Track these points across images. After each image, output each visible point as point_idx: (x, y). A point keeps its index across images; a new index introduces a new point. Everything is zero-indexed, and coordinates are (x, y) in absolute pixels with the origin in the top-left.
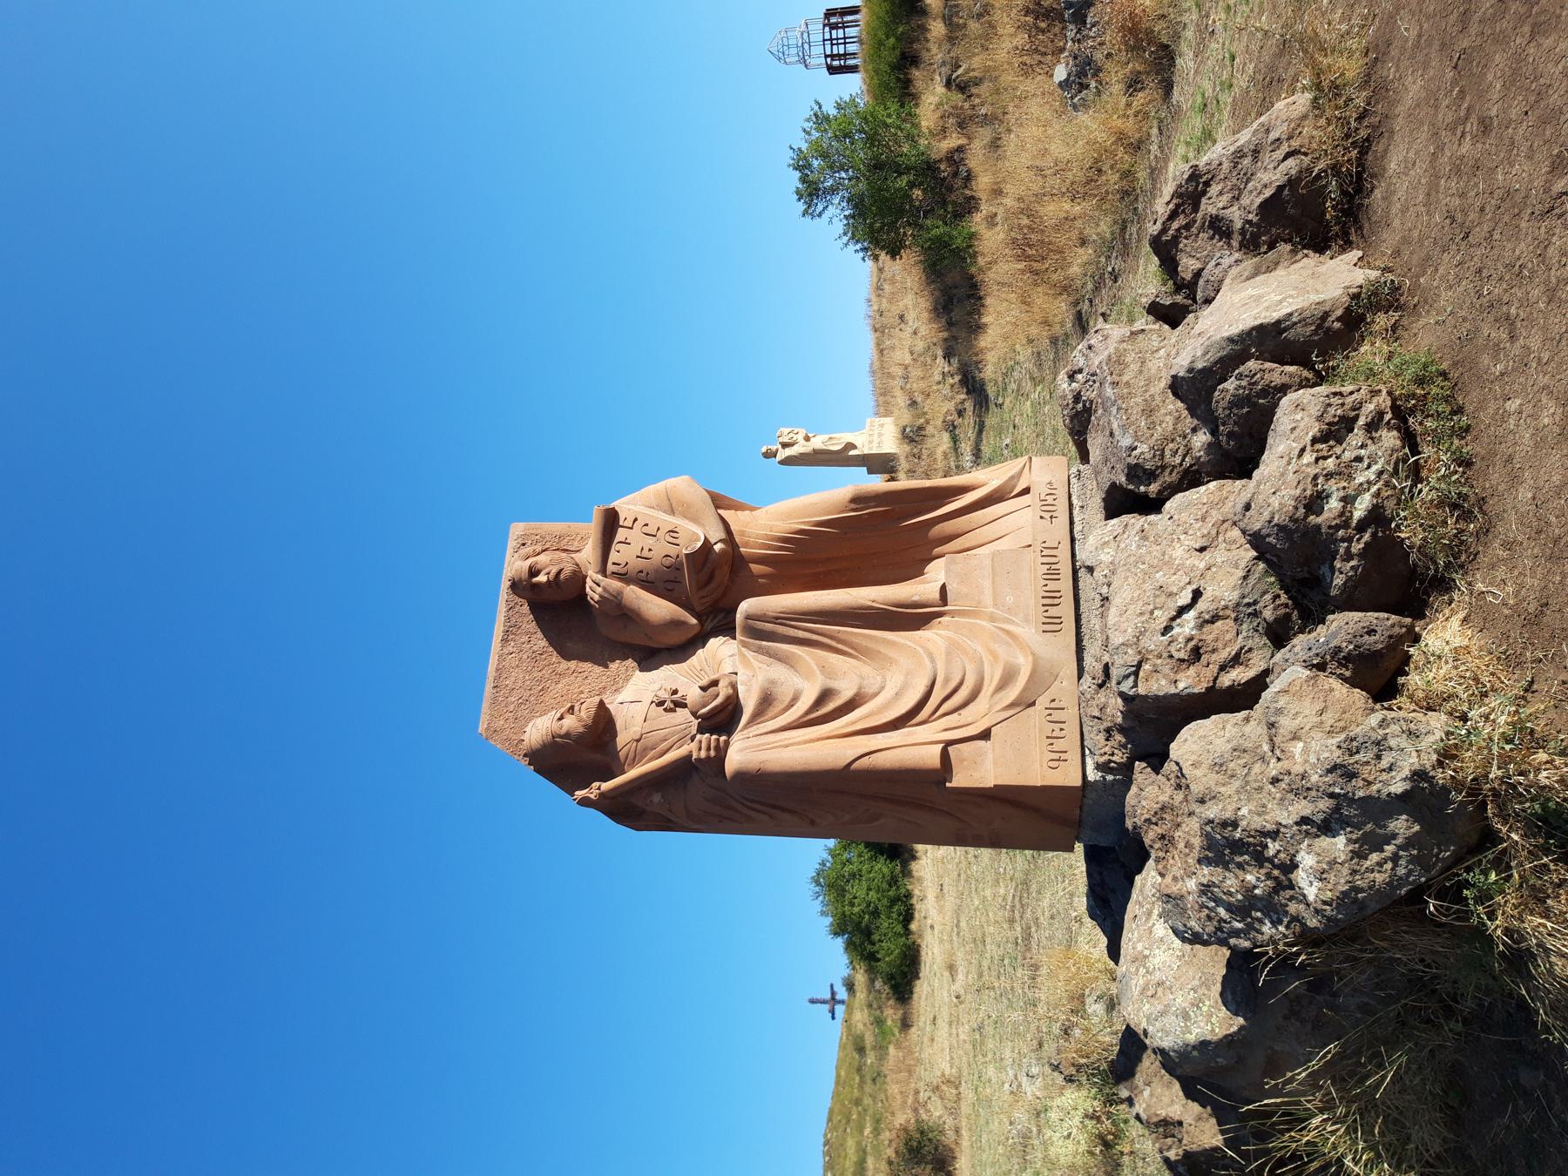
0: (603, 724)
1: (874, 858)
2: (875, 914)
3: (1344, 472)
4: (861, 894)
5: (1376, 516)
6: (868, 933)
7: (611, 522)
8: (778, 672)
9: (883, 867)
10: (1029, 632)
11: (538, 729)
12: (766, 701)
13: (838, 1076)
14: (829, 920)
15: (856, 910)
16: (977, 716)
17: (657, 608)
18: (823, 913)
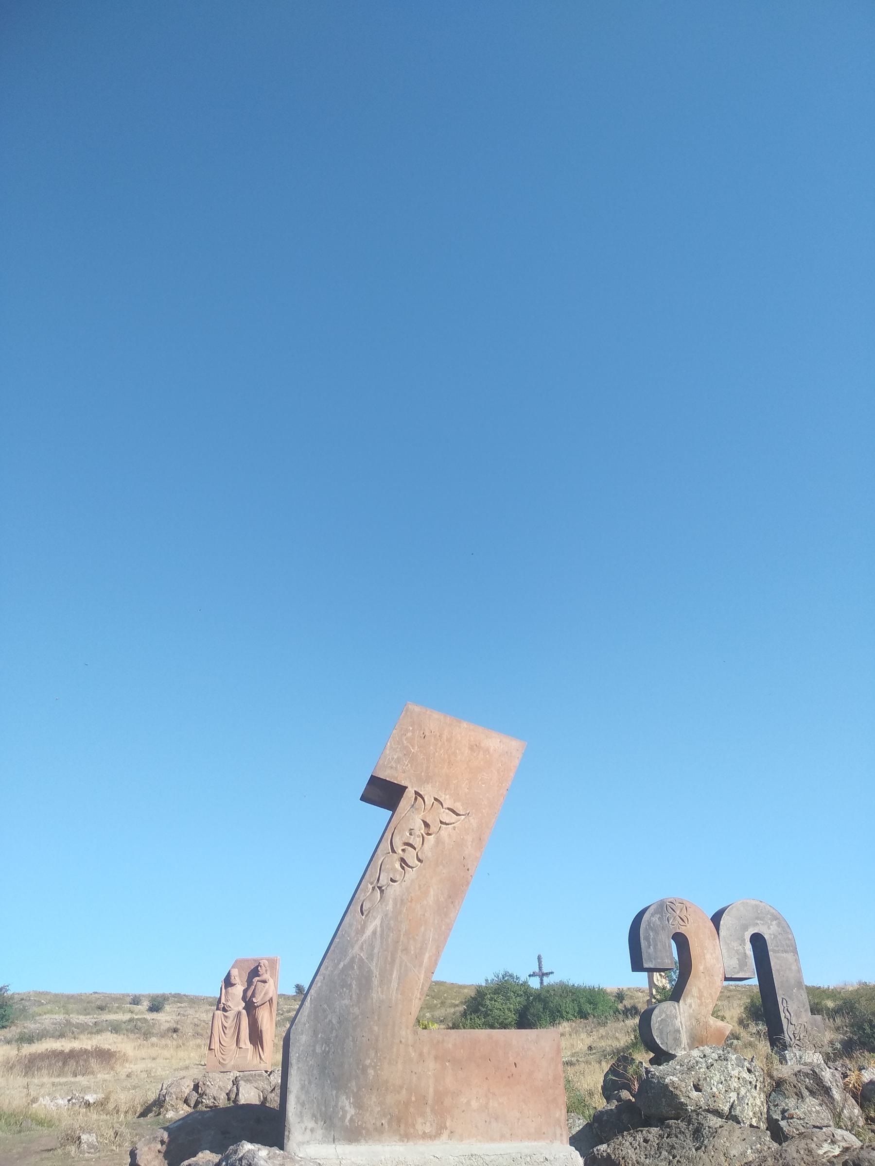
0: (233, 985)
1: (517, 1011)
2: (486, 1015)
3: (209, 1099)
4: (498, 1005)
5: (202, 1102)
6: (476, 1011)
7: (265, 982)
8: (232, 1018)
9: (512, 1017)
10: (232, 1063)
11: (235, 972)
12: (226, 1017)
13: (464, 987)
14: (484, 984)
15: (488, 1002)
16: (219, 1055)
17: (249, 993)
18: (487, 980)
